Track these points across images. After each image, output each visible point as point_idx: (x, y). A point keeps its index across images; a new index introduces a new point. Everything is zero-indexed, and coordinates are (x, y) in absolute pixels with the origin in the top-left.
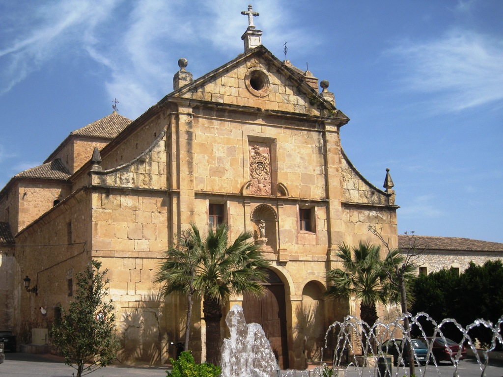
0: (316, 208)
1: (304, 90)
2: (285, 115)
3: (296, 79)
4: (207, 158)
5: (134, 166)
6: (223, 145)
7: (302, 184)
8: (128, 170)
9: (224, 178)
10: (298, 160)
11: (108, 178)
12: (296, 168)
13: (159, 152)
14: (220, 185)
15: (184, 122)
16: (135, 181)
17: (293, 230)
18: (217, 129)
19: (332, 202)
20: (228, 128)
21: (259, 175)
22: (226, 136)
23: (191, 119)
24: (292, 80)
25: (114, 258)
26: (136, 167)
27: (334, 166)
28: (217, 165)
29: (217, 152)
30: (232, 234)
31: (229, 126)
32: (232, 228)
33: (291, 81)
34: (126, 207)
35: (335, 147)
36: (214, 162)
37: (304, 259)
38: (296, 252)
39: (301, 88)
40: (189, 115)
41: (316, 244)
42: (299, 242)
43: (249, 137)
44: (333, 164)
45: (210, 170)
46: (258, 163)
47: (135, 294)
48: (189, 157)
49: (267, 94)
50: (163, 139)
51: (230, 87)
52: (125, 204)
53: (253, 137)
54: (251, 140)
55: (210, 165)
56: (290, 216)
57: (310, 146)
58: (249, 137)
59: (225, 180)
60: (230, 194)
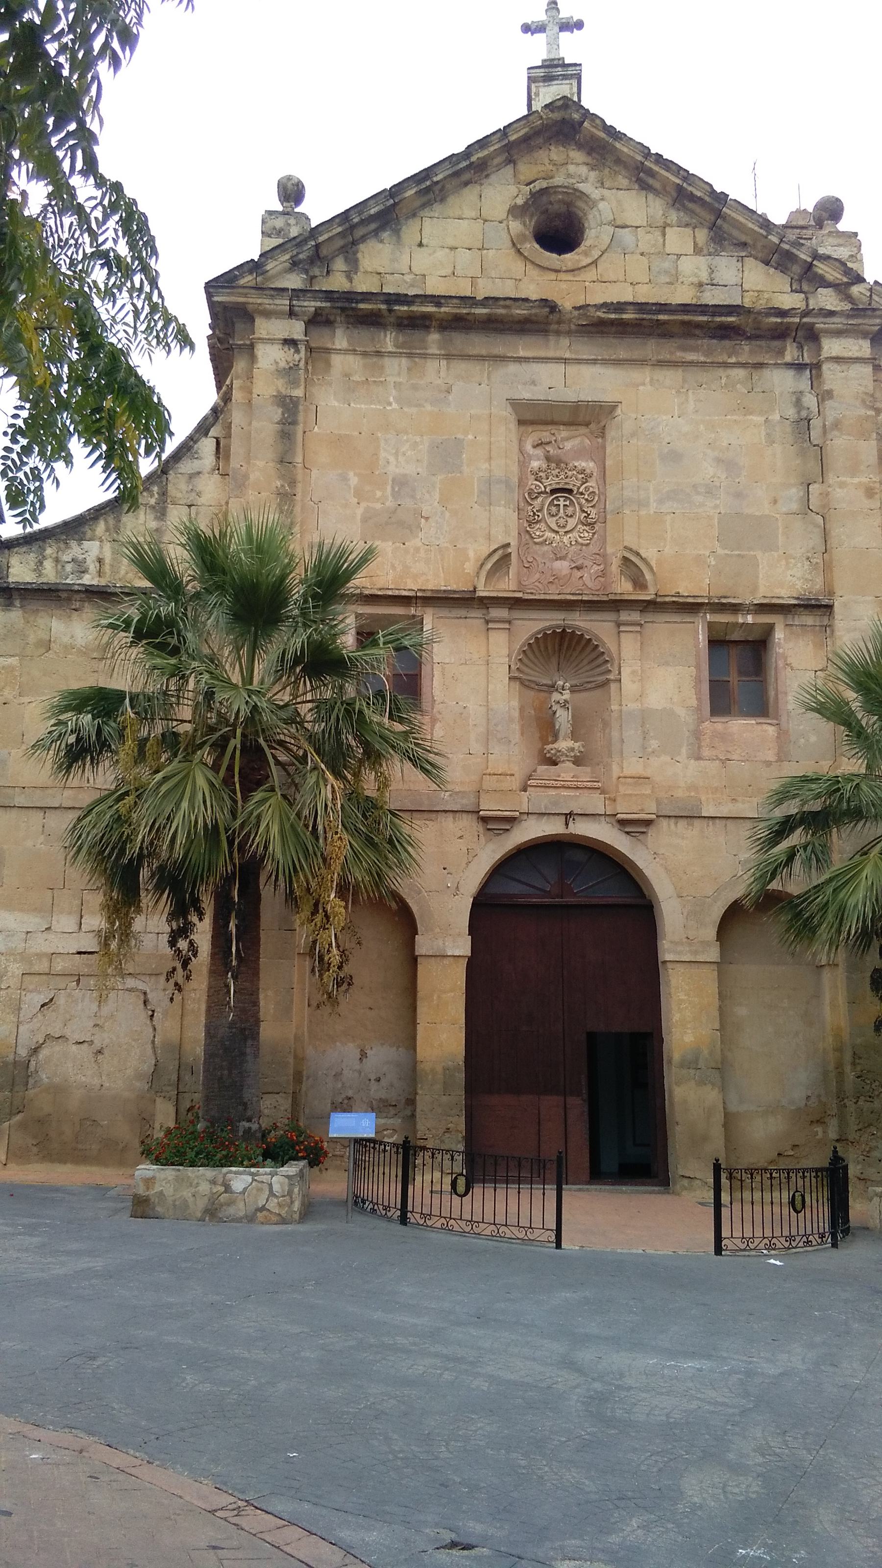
0: (779, 634)
1: (735, 233)
2: (655, 317)
3: (699, 194)
4: (354, 480)
5: (106, 521)
6: (418, 439)
7: (720, 551)
8: (84, 533)
9: (411, 543)
10: (708, 470)
11: (14, 561)
12: (699, 499)
13: (192, 476)
14: (399, 568)
15: (273, 368)
16: (107, 568)
17: (681, 712)
18: (397, 385)
19: (845, 605)
20: (439, 382)
21: (557, 532)
22: (429, 408)
23: (297, 357)
24: (691, 205)
25: (15, 811)
26: (111, 522)
27: (856, 480)
28: (390, 503)
29: (392, 459)
30: (438, 725)
31: (442, 374)
32: (438, 707)
33: (685, 209)
34: (68, 648)
35: (863, 412)
36: (379, 494)
37: (724, 811)
38: (693, 787)
39: (726, 226)
40: (290, 343)
41: (780, 760)
42: (706, 752)
43: (516, 404)
44: (854, 471)
45: (365, 520)
46: (553, 491)
47: (76, 928)
48: (282, 477)
49: (589, 260)
50: (210, 434)
51: (453, 249)
52: (66, 640)
53: (531, 405)
54: (528, 416)
55: (363, 505)
56: (667, 664)
57: (759, 419)
58: (516, 404)
59: (417, 550)
60: (429, 594)
